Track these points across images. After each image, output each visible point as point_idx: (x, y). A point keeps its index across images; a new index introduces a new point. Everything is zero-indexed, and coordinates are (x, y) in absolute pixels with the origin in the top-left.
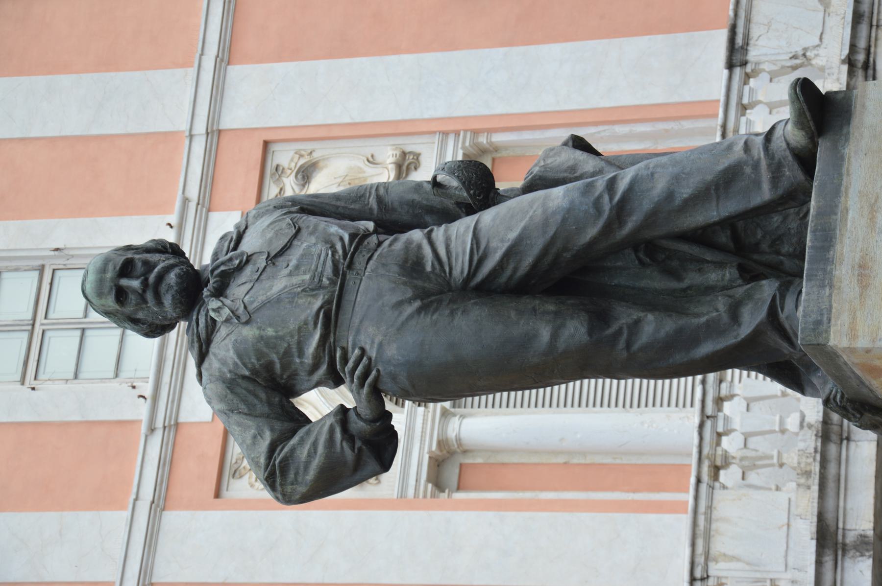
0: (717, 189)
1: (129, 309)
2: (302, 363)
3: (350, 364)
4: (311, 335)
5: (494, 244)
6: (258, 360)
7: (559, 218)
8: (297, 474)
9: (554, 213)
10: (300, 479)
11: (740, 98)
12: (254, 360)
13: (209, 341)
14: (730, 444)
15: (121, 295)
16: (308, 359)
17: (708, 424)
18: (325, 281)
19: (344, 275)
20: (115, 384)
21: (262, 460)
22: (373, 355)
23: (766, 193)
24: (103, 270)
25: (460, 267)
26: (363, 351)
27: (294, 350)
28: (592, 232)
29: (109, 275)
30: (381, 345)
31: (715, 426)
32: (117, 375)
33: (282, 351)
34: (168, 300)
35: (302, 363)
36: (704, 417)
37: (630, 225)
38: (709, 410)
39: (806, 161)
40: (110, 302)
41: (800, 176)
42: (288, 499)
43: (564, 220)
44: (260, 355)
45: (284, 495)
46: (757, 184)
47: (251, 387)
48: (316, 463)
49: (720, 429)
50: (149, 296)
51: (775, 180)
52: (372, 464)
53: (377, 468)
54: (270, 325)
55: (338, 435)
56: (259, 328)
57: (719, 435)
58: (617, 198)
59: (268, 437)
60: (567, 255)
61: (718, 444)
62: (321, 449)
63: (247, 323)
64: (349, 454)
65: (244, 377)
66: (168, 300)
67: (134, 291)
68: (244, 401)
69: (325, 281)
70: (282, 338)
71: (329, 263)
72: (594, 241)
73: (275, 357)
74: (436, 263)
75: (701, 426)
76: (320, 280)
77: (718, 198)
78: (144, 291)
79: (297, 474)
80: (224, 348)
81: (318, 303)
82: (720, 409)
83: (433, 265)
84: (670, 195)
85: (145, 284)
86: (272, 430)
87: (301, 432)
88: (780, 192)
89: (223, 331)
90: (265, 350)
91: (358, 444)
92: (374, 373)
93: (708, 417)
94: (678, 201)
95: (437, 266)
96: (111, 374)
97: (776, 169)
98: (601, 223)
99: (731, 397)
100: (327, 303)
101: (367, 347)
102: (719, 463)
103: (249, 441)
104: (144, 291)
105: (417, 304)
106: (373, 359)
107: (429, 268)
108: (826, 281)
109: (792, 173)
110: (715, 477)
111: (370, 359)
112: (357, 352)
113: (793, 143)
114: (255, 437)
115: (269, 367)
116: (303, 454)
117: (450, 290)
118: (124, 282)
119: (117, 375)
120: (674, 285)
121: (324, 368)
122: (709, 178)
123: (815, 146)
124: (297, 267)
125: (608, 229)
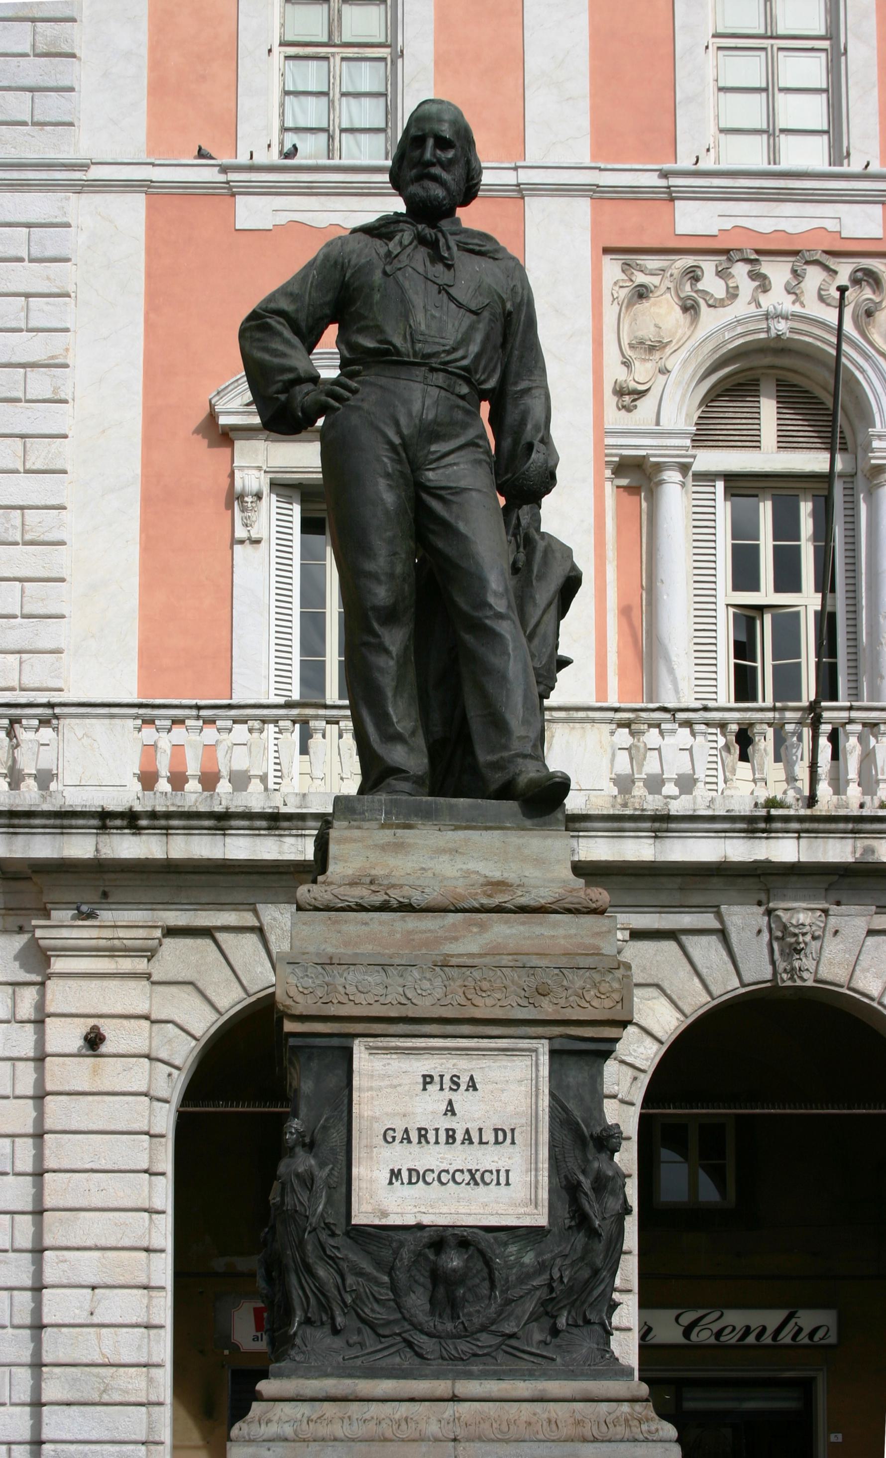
8: (259, 340)
10: (255, 344)
14: (652, 737)
17: (668, 716)
20: (713, 129)
22: (352, 403)
25: (432, 476)
30: (359, 408)
31: (666, 721)
32: (722, 131)
36: (673, 711)
38: (680, 715)
42: (243, 333)
48: (267, 357)
49: (663, 726)
57: (658, 726)
61: (650, 726)
62: (276, 361)
74: (439, 454)
75: (665, 709)
79: (259, 340)
82: (681, 725)
83: (435, 452)
87: (295, 340)
92: (337, 404)
93: (674, 715)
95: (435, 457)
96: (722, 126)
99: (693, 734)
101: (358, 396)
102: (633, 727)
106: (348, 403)
107: (433, 448)
110: (621, 724)
116: (277, 345)
117: (413, 471)
119: (722, 131)
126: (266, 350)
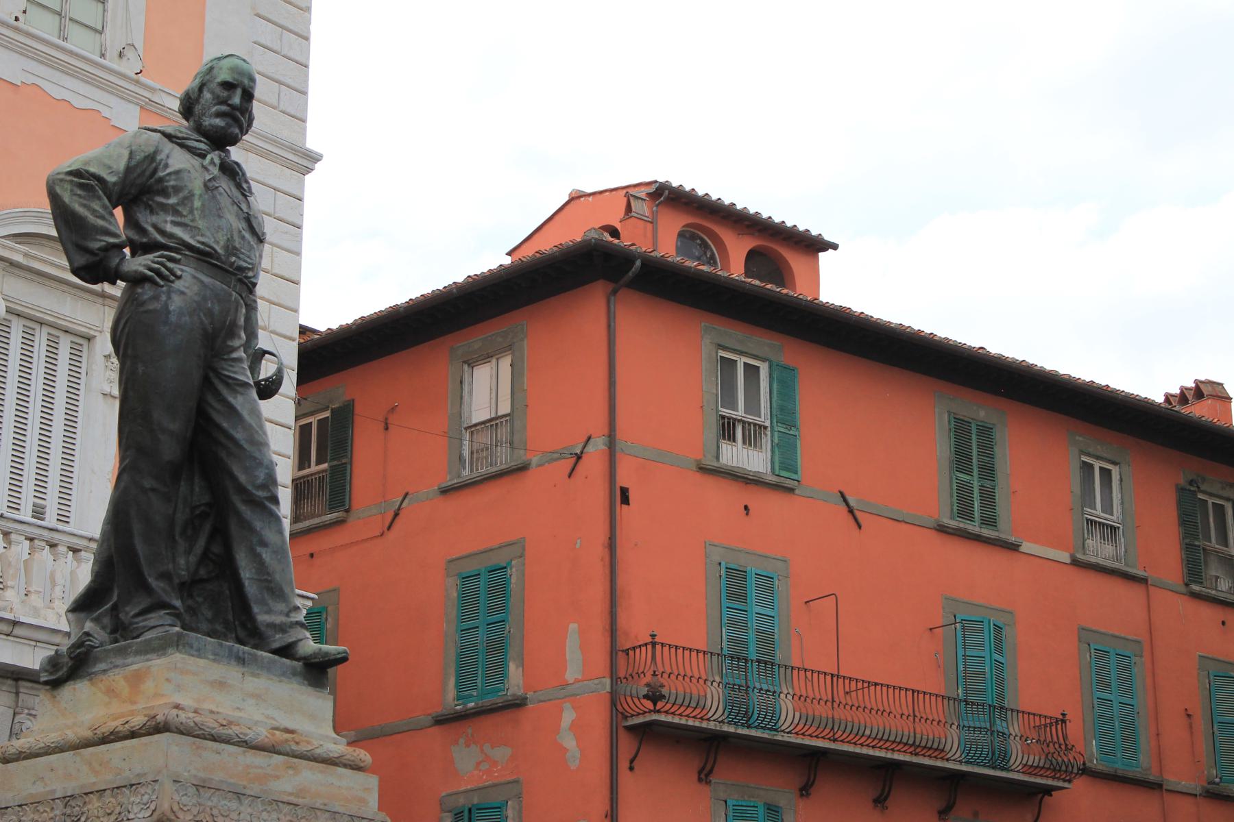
0: (266, 580)
1: (213, 85)
2: (166, 222)
3: (170, 265)
4: (192, 237)
5: (240, 398)
6: (173, 187)
7: (257, 454)
8: (80, 196)
9: (260, 451)
11: (19, 533)
12: (172, 183)
13: (182, 146)
15: (228, 86)
16: (169, 228)
18: (233, 259)
19: (235, 275)
21: (92, 169)
23: (262, 618)
24: (241, 73)
26: (179, 278)
27: (178, 219)
28: (243, 478)
29: (246, 82)
30: (183, 293)
33: (180, 209)
34: (219, 122)
35: (166, 222)
37: (243, 508)
39: (286, 651)
40: (224, 76)
41: (276, 645)
43: (255, 459)
44: (177, 190)
45: (61, 180)
46: (269, 612)
47: (148, 173)
50: (224, 108)
51: (272, 626)
52: (81, 260)
53: (76, 265)
54: (203, 205)
55: (112, 240)
56: (201, 196)
58: (267, 503)
59: (112, 179)
60: (223, 455)
62: (101, 222)
63: (205, 185)
64: (95, 245)
65: (155, 171)
66: (219, 122)
67: (230, 97)
68: (137, 166)
69: (233, 259)
70: (191, 212)
71: (245, 265)
72: (234, 478)
73: (173, 200)
76: (235, 255)
77: (260, 580)
78: (229, 105)
80: (178, 160)
81: (220, 251)
84: (264, 544)
85: (233, 107)
86: (115, 184)
88: (263, 629)
89: (196, 162)
90: (181, 195)
91: (102, 254)
94: (259, 549)
97: (282, 628)
98: (250, 488)
100: (218, 257)
103: (107, 162)
104: (229, 105)
105: (210, 330)
108: (217, 658)
109: (279, 640)
111: (172, 282)
112: (179, 273)
113: (301, 644)
114: (110, 167)
115: (164, 192)
116: (96, 206)
118: (239, 92)
120: (178, 530)
121: (160, 238)
122: (277, 577)
123: (298, 660)
124: (243, 238)
125: (242, 490)
126: (84, 206)
